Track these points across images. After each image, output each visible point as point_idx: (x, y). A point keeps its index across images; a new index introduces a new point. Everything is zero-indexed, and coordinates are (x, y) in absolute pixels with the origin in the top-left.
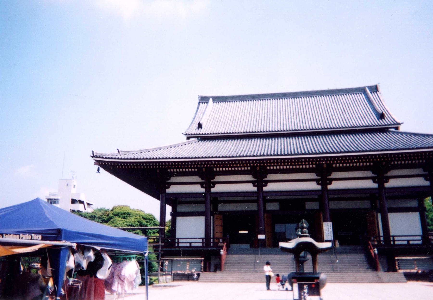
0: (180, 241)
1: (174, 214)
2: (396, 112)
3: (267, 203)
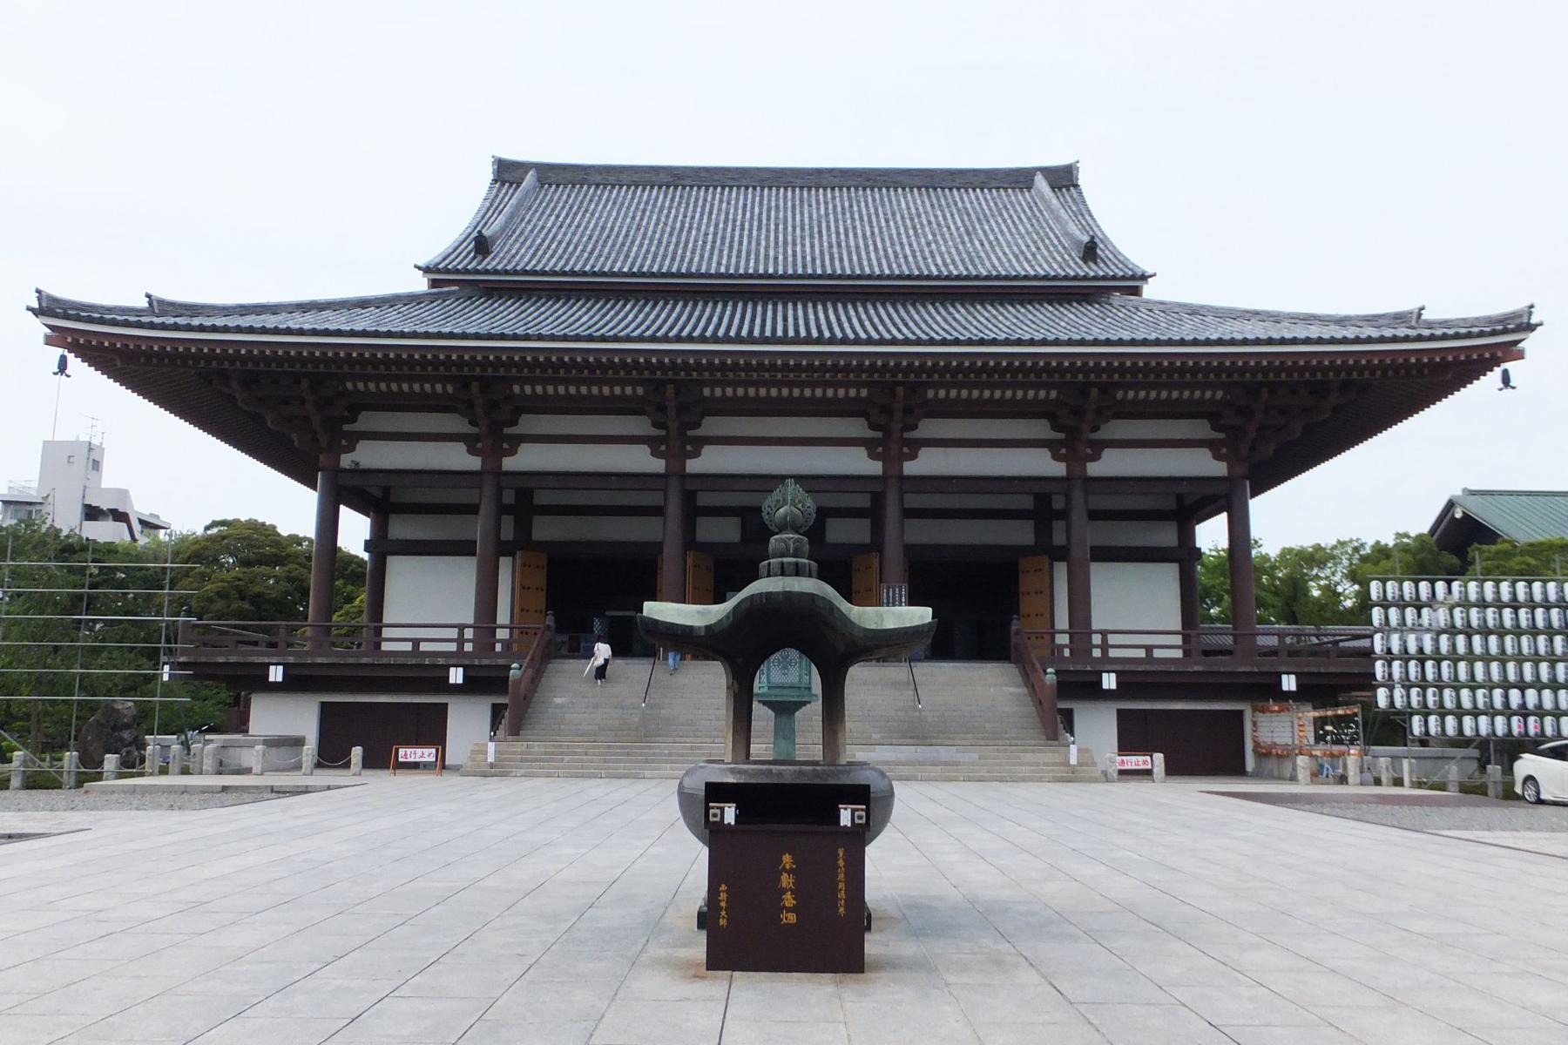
2: (1130, 237)
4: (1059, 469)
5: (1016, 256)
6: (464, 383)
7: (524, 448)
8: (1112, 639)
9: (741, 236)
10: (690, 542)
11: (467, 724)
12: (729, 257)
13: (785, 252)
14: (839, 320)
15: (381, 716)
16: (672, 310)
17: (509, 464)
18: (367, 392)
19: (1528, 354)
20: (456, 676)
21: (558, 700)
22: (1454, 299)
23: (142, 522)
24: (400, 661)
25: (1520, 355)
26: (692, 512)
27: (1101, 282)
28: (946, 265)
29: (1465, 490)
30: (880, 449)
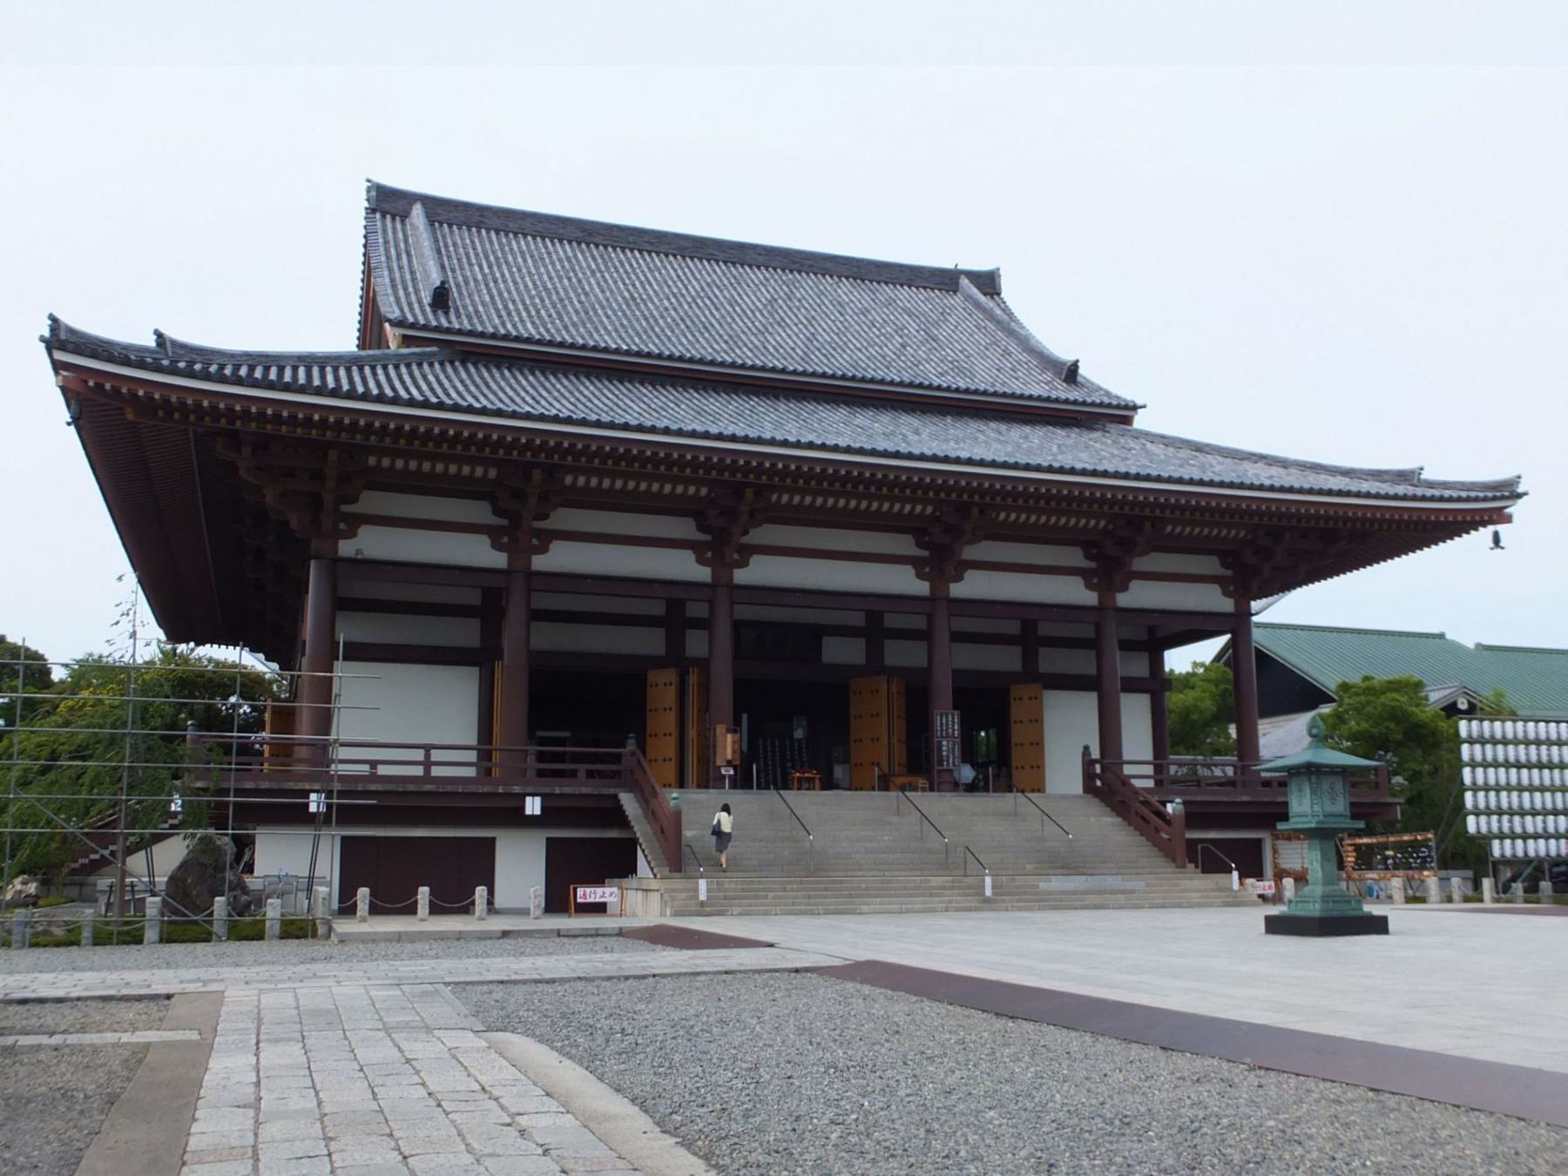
0: (436, 755)
3: (663, 630)
19: (1515, 519)
22: (1451, 461)
25: (1508, 519)
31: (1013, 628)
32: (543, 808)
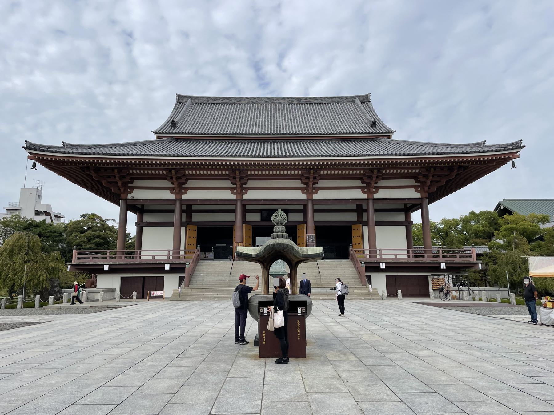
1: (140, 226)
4: (364, 196)
5: (350, 126)
6: (170, 171)
7: (189, 191)
8: (383, 252)
9: (259, 121)
10: (244, 222)
11: (171, 283)
12: (256, 128)
13: (274, 126)
14: (292, 149)
15: (141, 282)
16: (237, 146)
17: (184, 197)
18: (137, 174)
20: (167, 267)
21: (202, 275)
22: (496, 137)
23: (55, 216)
24: (149, 262)
25: (518, 157)
26: (245, 211)
27: (377, 134)
28: (326, 130)
29: (504, 199)
30: (306, 191)
31: (354, 207)
32: (170, 268)
